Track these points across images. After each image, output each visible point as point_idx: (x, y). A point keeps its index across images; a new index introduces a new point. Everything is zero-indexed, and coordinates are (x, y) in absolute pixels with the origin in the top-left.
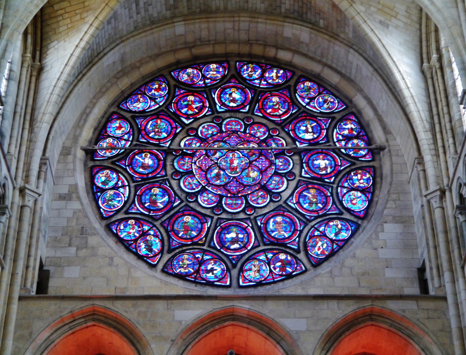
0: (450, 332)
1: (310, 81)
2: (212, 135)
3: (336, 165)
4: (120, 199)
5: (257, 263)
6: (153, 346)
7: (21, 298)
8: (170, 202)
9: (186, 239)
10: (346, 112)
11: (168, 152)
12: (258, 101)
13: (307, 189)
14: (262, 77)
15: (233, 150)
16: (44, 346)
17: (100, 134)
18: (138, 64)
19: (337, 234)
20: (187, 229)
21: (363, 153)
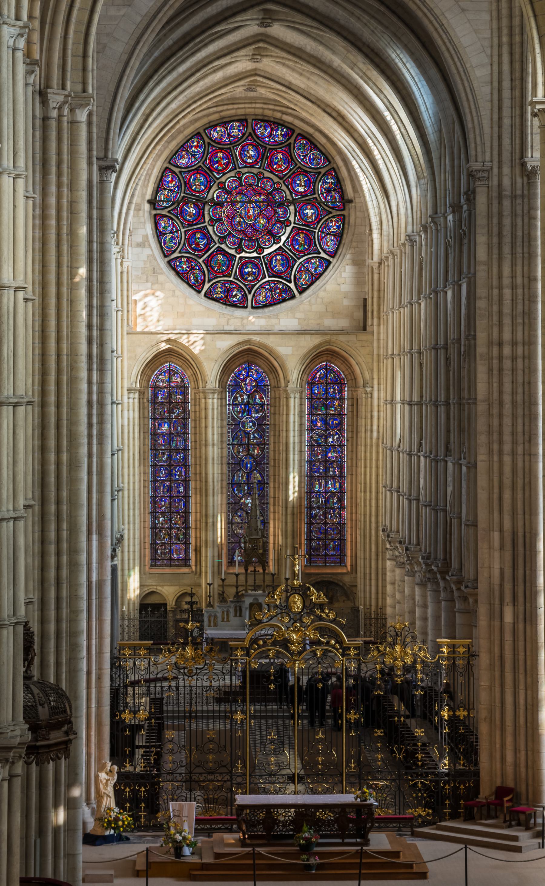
0: (373, 355)
2: (236, 188)
3: (318, 214)
4: (175, 241)
5: (264, 290)
6: (205, 364)
7: (127, 334)
9: (219, 272)
10: (329, 167)
12: (267, 158)
13: (297, 234)
14: (270, 135)
15: (250, 202)
17: (158, 187)
18: (182, 129)
19: (315, 269)
20: (220, 265)
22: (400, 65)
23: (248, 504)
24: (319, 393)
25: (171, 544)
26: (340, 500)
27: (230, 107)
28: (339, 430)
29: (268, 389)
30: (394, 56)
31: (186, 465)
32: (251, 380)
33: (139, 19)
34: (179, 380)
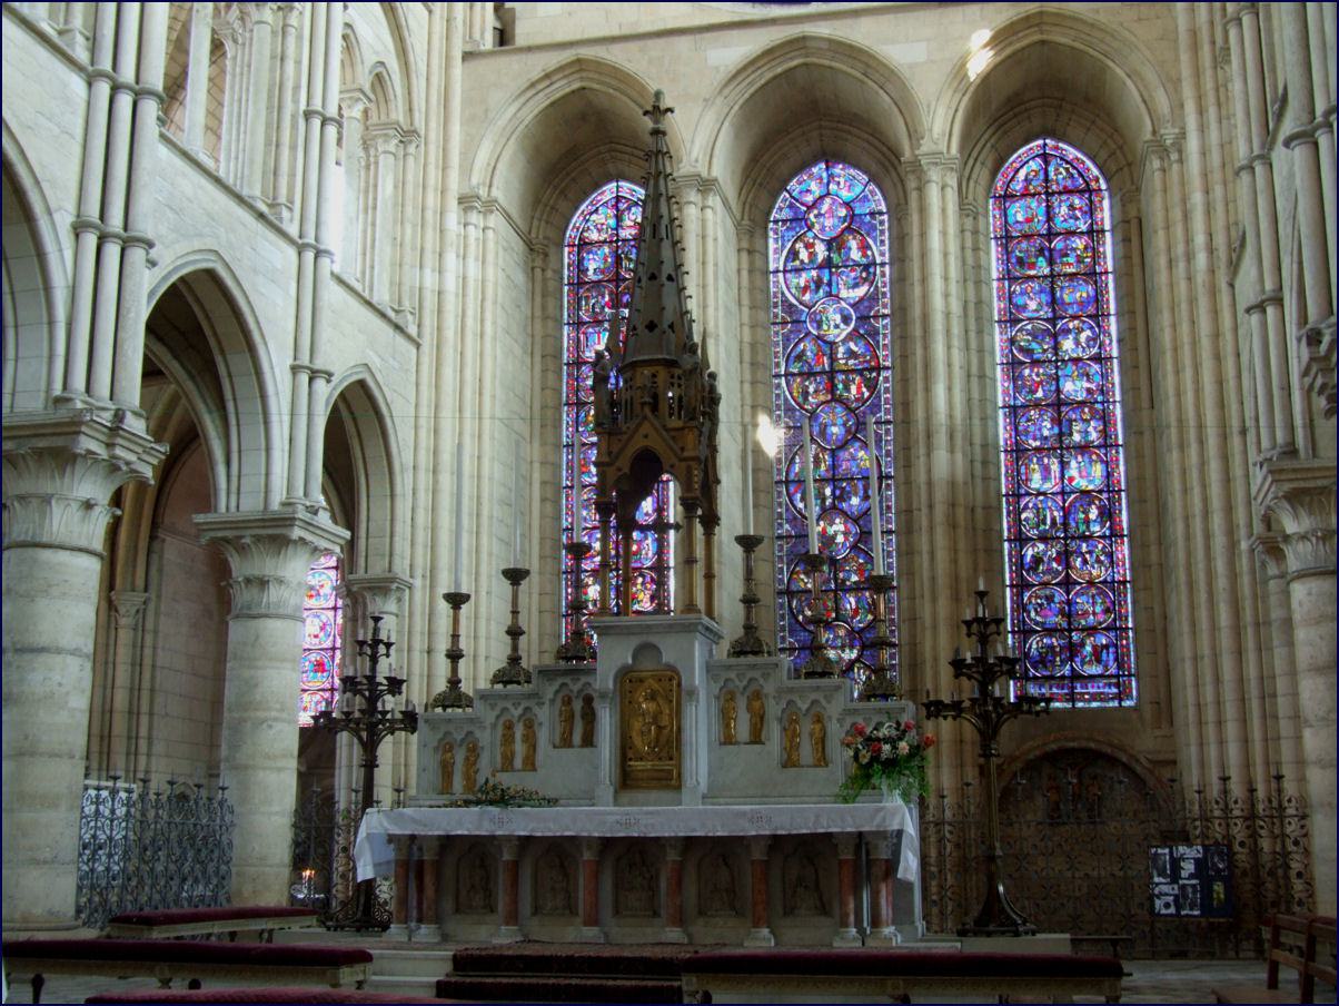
0: (1176, 40)
16: (509, 130)
23: (834, 537)
24: (1029, 220)
26: (1108, 514)
28: (1093, 317)
29: (882, 223)
32: (834, 201)
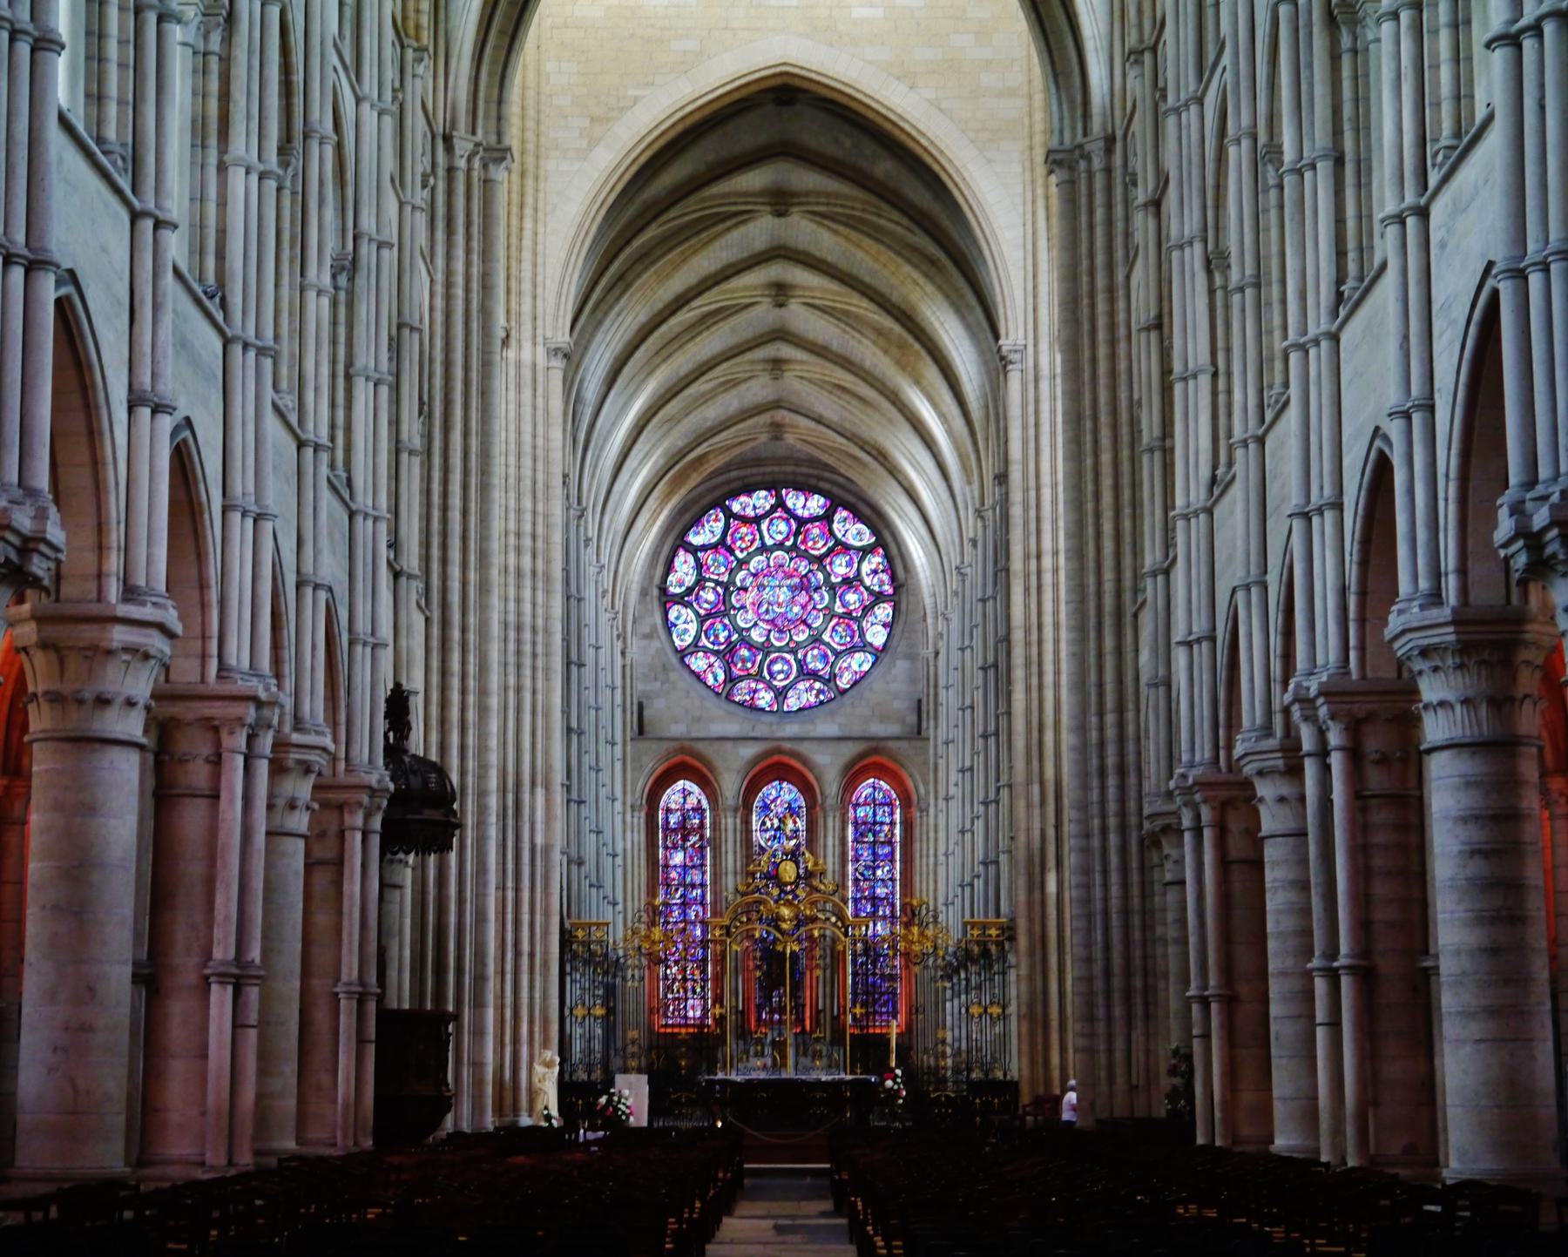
1: (845, 508)
8: (729, 636)
11: (726, 586)
15: (780, 587)
19: (860, 666)
20: (744, 661)
21: (886, 587)
22: (937, 325)
24: (866, 816)
25: (686, 1000)
27: (755, 470)
30: (928, 313)
31: (703, 904)
33: (596, 175)
34: (695, 802)
